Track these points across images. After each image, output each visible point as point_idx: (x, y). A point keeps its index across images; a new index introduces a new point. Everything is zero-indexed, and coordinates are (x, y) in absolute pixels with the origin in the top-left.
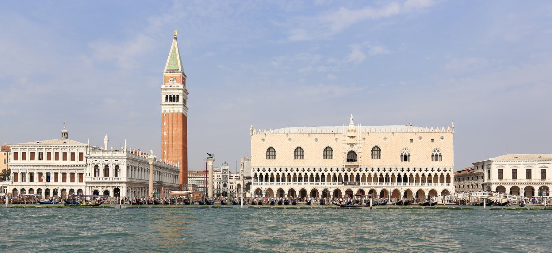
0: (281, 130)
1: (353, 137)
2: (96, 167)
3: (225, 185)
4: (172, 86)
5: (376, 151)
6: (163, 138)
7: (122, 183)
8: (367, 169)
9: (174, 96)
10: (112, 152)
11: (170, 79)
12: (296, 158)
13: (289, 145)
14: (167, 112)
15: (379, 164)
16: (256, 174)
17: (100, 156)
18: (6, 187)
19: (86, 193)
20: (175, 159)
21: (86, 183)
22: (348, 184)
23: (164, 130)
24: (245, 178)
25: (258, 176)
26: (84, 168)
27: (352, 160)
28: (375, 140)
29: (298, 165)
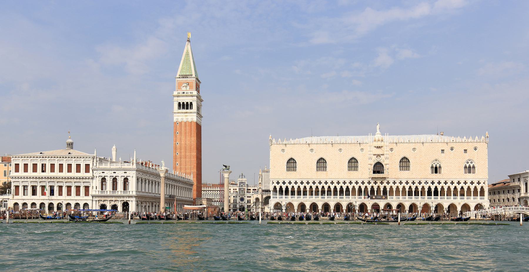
0: (302, 140)
1: (380, 147)
2: (104, 180)
3: (242, 199)
4: (185, 93)
5: (405, 163)
6: (176, 148)
7: (132, 197)
8: (394, 181)
9: (187, 103)
10: (120, 164)
11: (183, 85)
12: (319, 170)
13: (311, 156)
14: (180, 120)
15: (408, 176)
16: (275, 187)
17: (108, 168)
18: (7, 201)
19: (92, 207)
20: (188, 171)
21: (93, 197)
22: (374, 197)
23: (176, 140)
24: (263, 191)
25: (278, 189)
27: (378, 172)
28: (404, 151)
29: (320, 178)
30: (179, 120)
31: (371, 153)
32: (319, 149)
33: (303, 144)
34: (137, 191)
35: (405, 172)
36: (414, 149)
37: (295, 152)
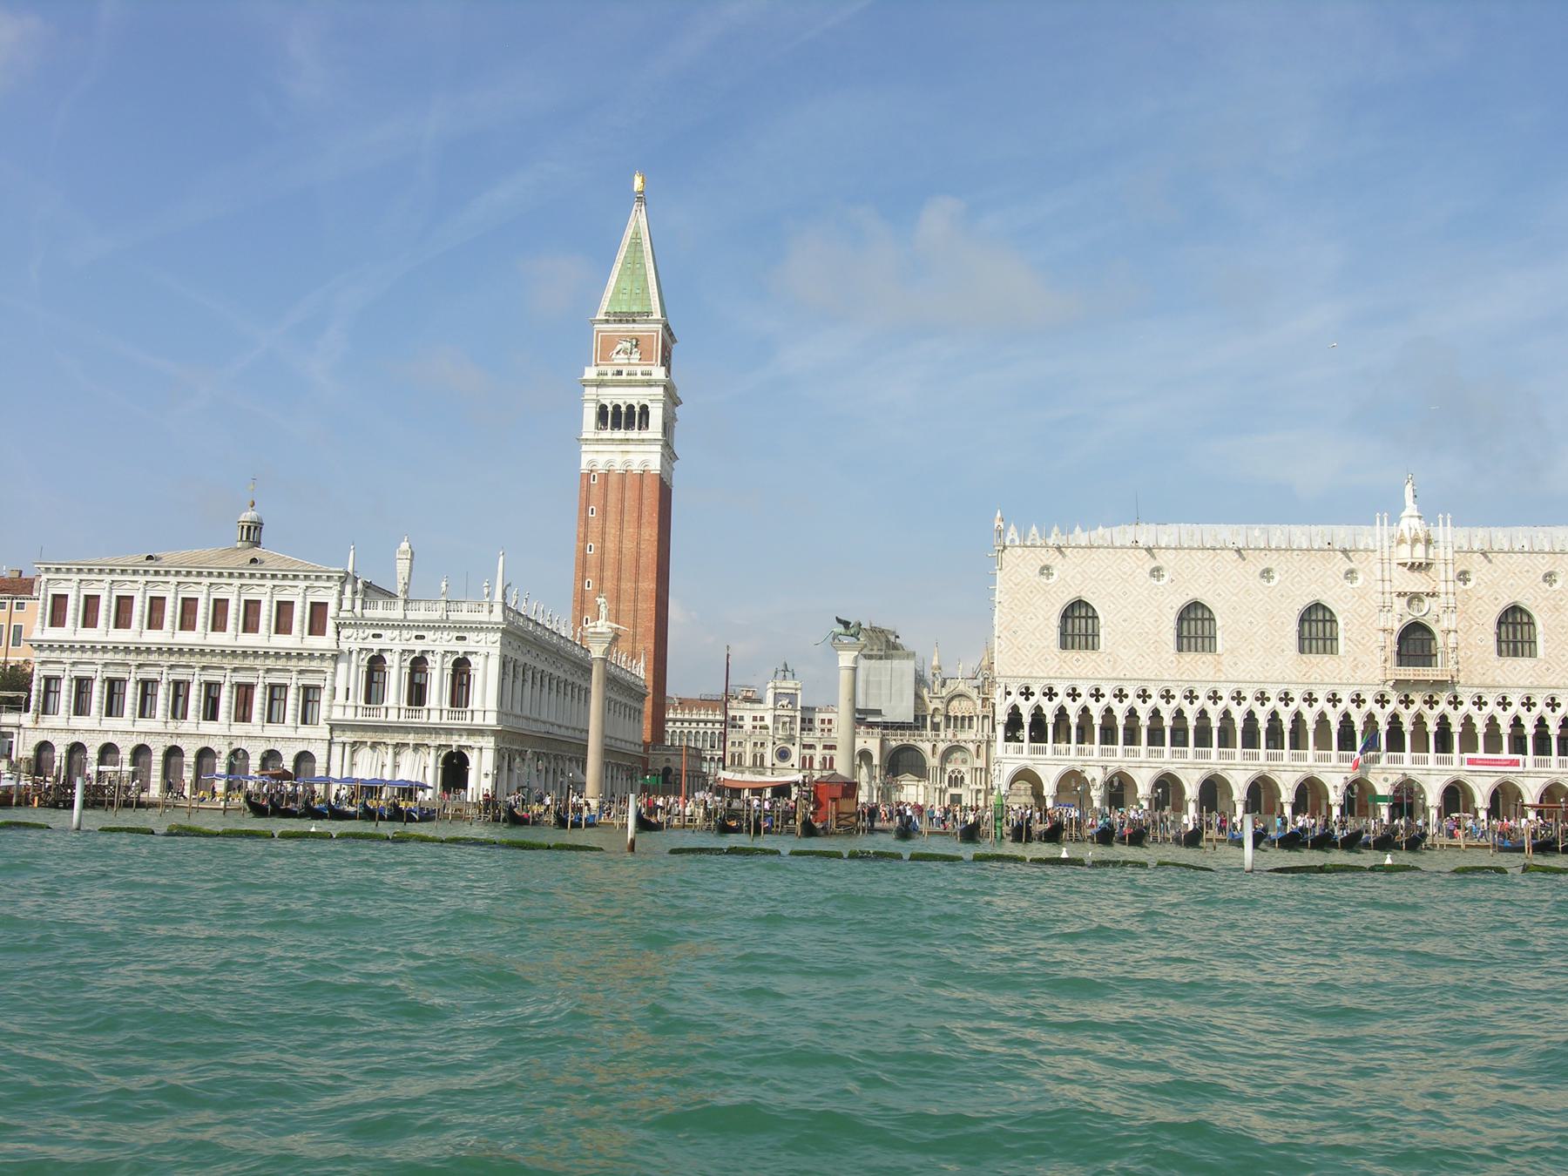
0: (1124, 534)
1: (1420, 564)
2: (376, 664)
4: (624, 373)
6: (583, 564)
7: (480, 732)
9: (630, 407)
10: (443, 605)
13: (1156, 594)
14: (601, 467)
17: (396, 620)
21: (332, 728)
23: (586, 536)
26: (327, 666)
28: (1511, 581)
29: (1193, 678)
30: (599, 467)
31: (1387, 588)
32: (1187, 568)
33: (1122, 547)
34: (502, 713)
35: (1523, 664)
36: (1549, 577)
37: (1093, 576)
